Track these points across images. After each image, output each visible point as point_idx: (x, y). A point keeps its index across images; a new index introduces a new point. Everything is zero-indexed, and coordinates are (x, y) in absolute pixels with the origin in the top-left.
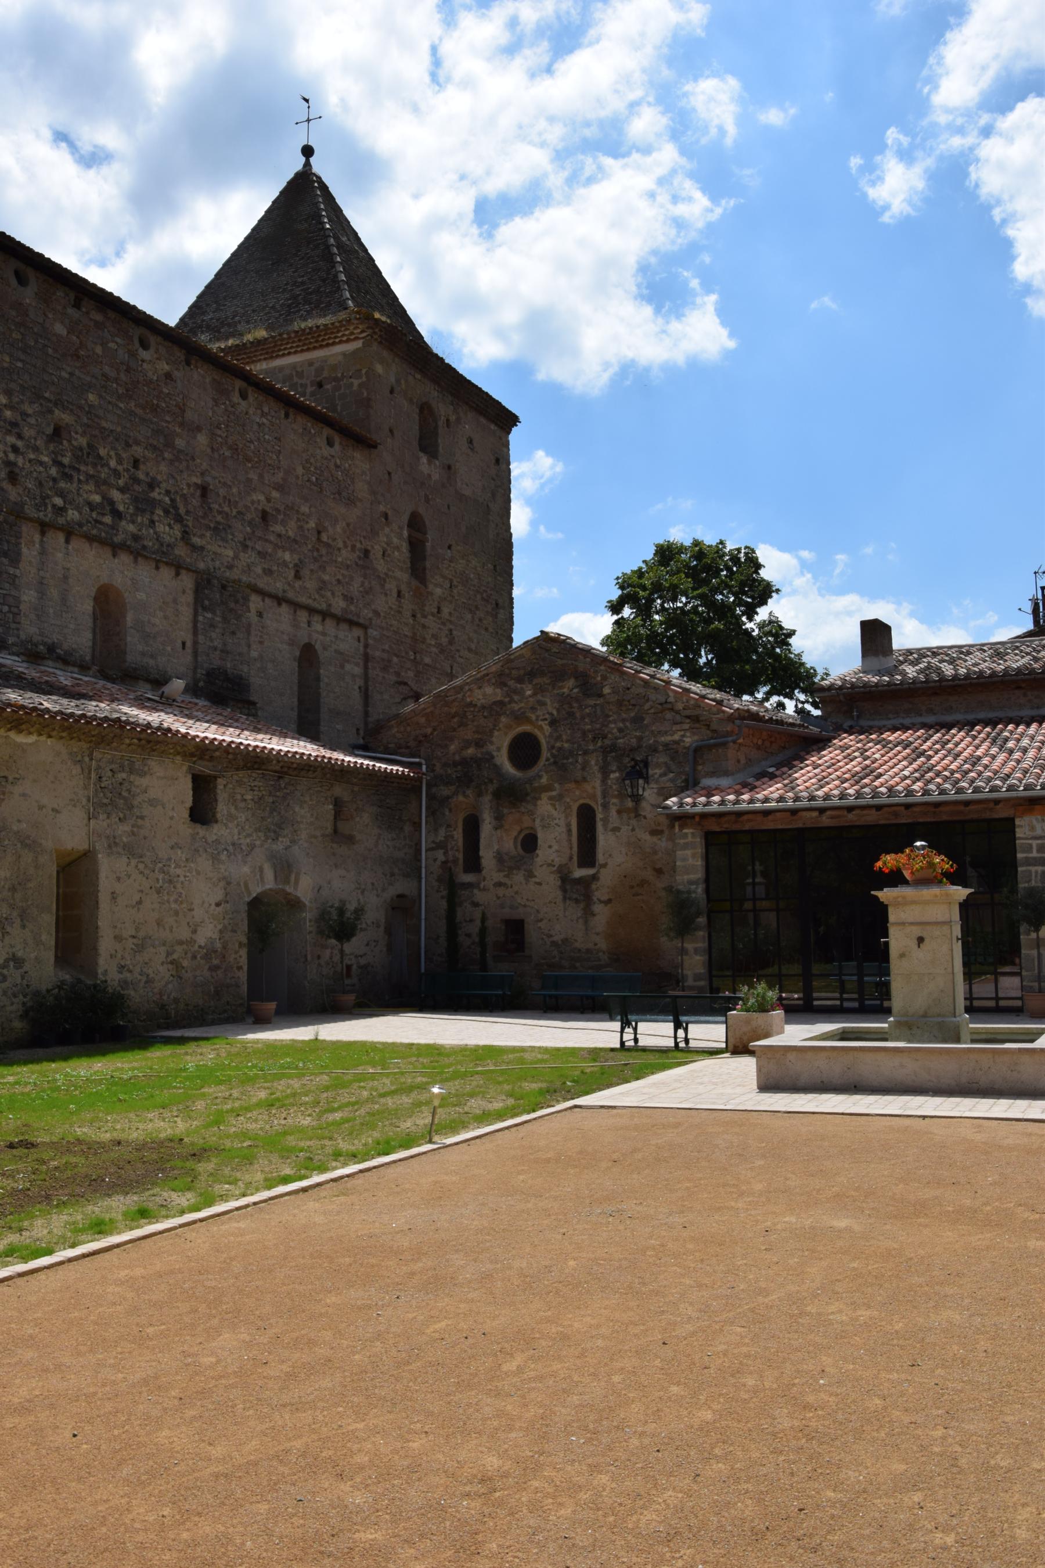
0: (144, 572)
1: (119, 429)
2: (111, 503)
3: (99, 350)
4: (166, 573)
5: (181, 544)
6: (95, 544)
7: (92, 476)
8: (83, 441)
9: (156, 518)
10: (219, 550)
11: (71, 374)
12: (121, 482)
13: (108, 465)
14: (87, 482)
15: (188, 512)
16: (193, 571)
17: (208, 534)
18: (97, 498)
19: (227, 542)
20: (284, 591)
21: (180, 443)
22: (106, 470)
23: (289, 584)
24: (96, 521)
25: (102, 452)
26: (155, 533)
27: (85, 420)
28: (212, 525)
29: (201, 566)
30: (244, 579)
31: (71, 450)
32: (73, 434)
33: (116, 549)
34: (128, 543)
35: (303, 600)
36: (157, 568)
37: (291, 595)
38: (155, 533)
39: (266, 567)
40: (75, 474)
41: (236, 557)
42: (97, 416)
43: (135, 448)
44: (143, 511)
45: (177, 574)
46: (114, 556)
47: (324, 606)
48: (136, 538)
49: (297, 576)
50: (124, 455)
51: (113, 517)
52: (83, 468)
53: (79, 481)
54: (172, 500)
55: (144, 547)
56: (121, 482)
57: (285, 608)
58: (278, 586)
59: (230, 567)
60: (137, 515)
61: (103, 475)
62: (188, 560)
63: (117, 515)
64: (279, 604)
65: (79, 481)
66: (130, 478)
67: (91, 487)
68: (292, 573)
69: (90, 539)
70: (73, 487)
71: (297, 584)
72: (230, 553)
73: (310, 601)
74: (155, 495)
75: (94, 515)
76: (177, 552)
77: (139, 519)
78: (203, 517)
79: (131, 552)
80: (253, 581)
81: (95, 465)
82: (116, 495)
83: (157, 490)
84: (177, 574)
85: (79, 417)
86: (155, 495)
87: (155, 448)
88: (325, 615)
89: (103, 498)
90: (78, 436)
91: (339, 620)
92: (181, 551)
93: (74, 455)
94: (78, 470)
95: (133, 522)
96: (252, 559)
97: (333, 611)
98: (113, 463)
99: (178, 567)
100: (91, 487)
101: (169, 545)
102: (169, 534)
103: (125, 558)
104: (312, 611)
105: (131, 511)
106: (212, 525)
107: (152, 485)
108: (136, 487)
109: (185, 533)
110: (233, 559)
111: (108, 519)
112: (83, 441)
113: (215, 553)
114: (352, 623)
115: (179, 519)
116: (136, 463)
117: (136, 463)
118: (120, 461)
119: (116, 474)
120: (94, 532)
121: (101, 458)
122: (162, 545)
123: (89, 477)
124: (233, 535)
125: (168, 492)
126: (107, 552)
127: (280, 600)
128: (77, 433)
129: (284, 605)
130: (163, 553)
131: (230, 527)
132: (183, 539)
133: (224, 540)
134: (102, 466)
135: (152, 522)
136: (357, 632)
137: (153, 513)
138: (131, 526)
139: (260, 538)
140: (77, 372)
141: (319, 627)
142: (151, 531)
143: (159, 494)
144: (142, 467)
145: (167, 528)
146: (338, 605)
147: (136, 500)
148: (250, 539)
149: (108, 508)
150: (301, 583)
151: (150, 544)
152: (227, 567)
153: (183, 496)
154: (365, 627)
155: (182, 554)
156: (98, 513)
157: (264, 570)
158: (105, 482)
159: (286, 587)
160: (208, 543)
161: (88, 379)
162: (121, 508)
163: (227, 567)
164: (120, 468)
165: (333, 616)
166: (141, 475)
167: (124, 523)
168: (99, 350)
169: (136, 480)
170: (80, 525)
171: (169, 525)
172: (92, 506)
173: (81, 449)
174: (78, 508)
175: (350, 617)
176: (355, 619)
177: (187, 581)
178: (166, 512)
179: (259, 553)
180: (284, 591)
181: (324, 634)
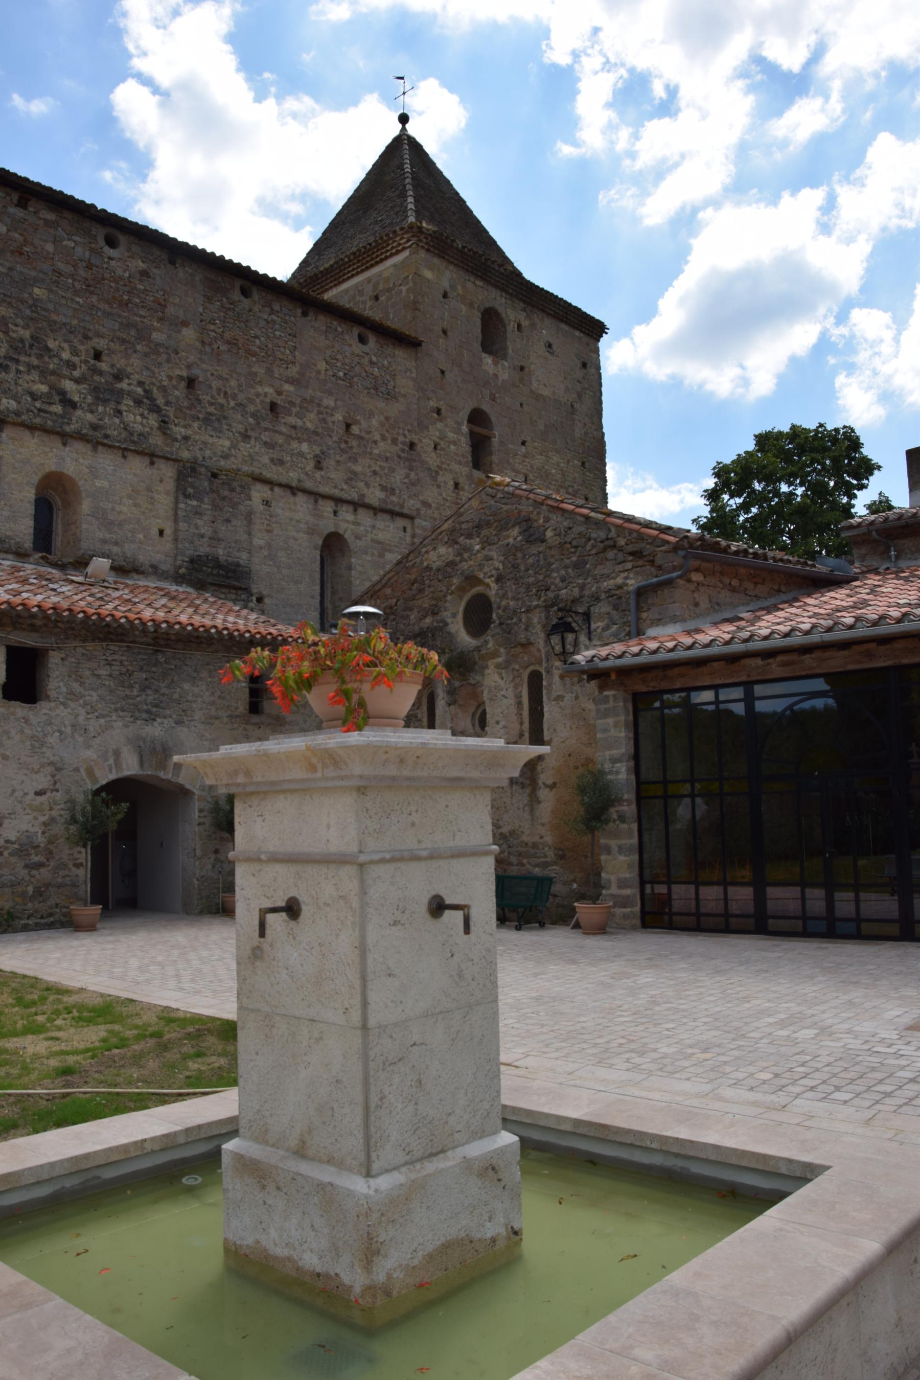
0: (106, 461)
1: (75, 322)
2: (62, 393)
3: (50, 247)
4: (137, 465)
5: (158, 433)
6: (37, 433)
7: (35, 367)
8: (26, 334)
9: (124, 408)
10: (211, 440)
11: (11, 269)
12: (76, 374)
13: (58, 356)
14: (28, 372)
15: (168, 403)
16: (175, 460)
17: (196, 425)
18: (44, 388)
19: (220, 432)
20: (299, 481)
21: (155, 335)
22: (56, 360)
23: (307, 474)
24: (40, 410)
25: (51, 344)
26: (122, 422)
27: (28, 312)
28: (201, 416)
29: (185, 455)
30: (245, 468)
31: (7, 341)
32: (10, 325)
33: (65, 438)
34: (84, 431)
35: (325, 489)
36: (124, 457)
37: (309, 485)
38: (122, 422)
39: (275, 456)
40: (13, 366)
41: (234, 446)
42: (46, 310)
43: (96, 340)
44: (105, 402)
45: (152, 463)
46: (65, 444)
47: (355, 496)
48: (95, 427)
49: (318, 466)
50: (81, 348)
51: (64, 406)
52: (23, 358)
53: (18, 371)
54: (145, 391)
55: (106, 436)
56: (76, 374)
57: (301, 498)
58: (293, 477)
59: (226, 457)
60: (98, 405)
61: (51, 366)
62: (168, 449)
63: (69, 403)
64: (294, 494)
65: (18, 371)
66: (89, 369)
67: (35, 376)
68: (311, 465)
69: (31, 428)
70: (10, 377)
71: (318, 475)
72: (227, 443)
73: (336, 492)
74: (124, 385)
75: (38, 404)
76: (151, 441)
77: (100, 409)
78: (189, 408)
79: (88, 441)
80: (257, 471)
81: (39, 357)
82: (68, 385)
83: (126, 381)
84: (152, 463)
85: (20, 310)
86: (124, 385)
87: (124, 341)
88: (356, 505)
89: (51, 388)
90: (19, 329)
91: (376, 510)
92: (157, 440)
93: (11, 346)
94: (17, 361)
95: (92, 412)
96: (257, 449)
97: (367, 501)
98: (65, 355)
99: (152, 457)
100: (35, 376)
101: (140, 435)
102: (141, 424)
103: (79, 446)
104: (338, 501)
105: (89, 399)
106: (201, 416)
107: (118, 377)
108: (96, 378)
109: (164, 423)
110: (230, 449)
111: (57, 409)
112: (26, 334)
113: (204, 443)
114: (393, 514)
115: (155, 409)
116: (98, 356)
117: (98, 356)
118: (75, 352)
119: (71, 366)
120: (38, 420)
121: (48, 350)
122: (132, 434)
123: (30, 367)
124: (230, 425)
125: (140, 384)
126: (57, 442)
127: (293, 490)
128: (16, 325)
129: (300, 494)
130: (133, 442)
131: (225, 418)
132: (159, 428)
133: (215, 429)
134: (50, 357)
135: (119, 412)
136: (401, 522)
137: (118, 403)
138: (89, 416)
139: (266, 429)
140: (19, 267)
141: (350, 517)
142: (117, 421)
143: (130, 384)
144: (104, 358)
145: (139, 418)
146: (375, 496)
147: (95, 390)
148: (252, 429)
149: (57, 398)
150: (323, 473)
151: (115, 433)
152: (221, 457)
153: (163, 389)
154: (411, 518)
155: (159, 443)
156: (43, 402)
157: (272, 460)
158: (53, 373)
159: (303, 477)
160: (196, 433)
161: (33, 273)
162: (76, 398)
163: (221, 457)
164: (75, 359)
165: (368, 507)
166: (103, 366)
167: (79, 413)
168: (50, 247)
169: (95, 371)
170: (18, 414)
171: (142, 415)
172: (34, 396)
173: (22, 340)
174: (15, 397)
175: (390, 507)
176: (397, 509)
177: (168, 471)
178: (138, 402)
179: (266, 443)
180: (299, 481)
181: (357, 524)
